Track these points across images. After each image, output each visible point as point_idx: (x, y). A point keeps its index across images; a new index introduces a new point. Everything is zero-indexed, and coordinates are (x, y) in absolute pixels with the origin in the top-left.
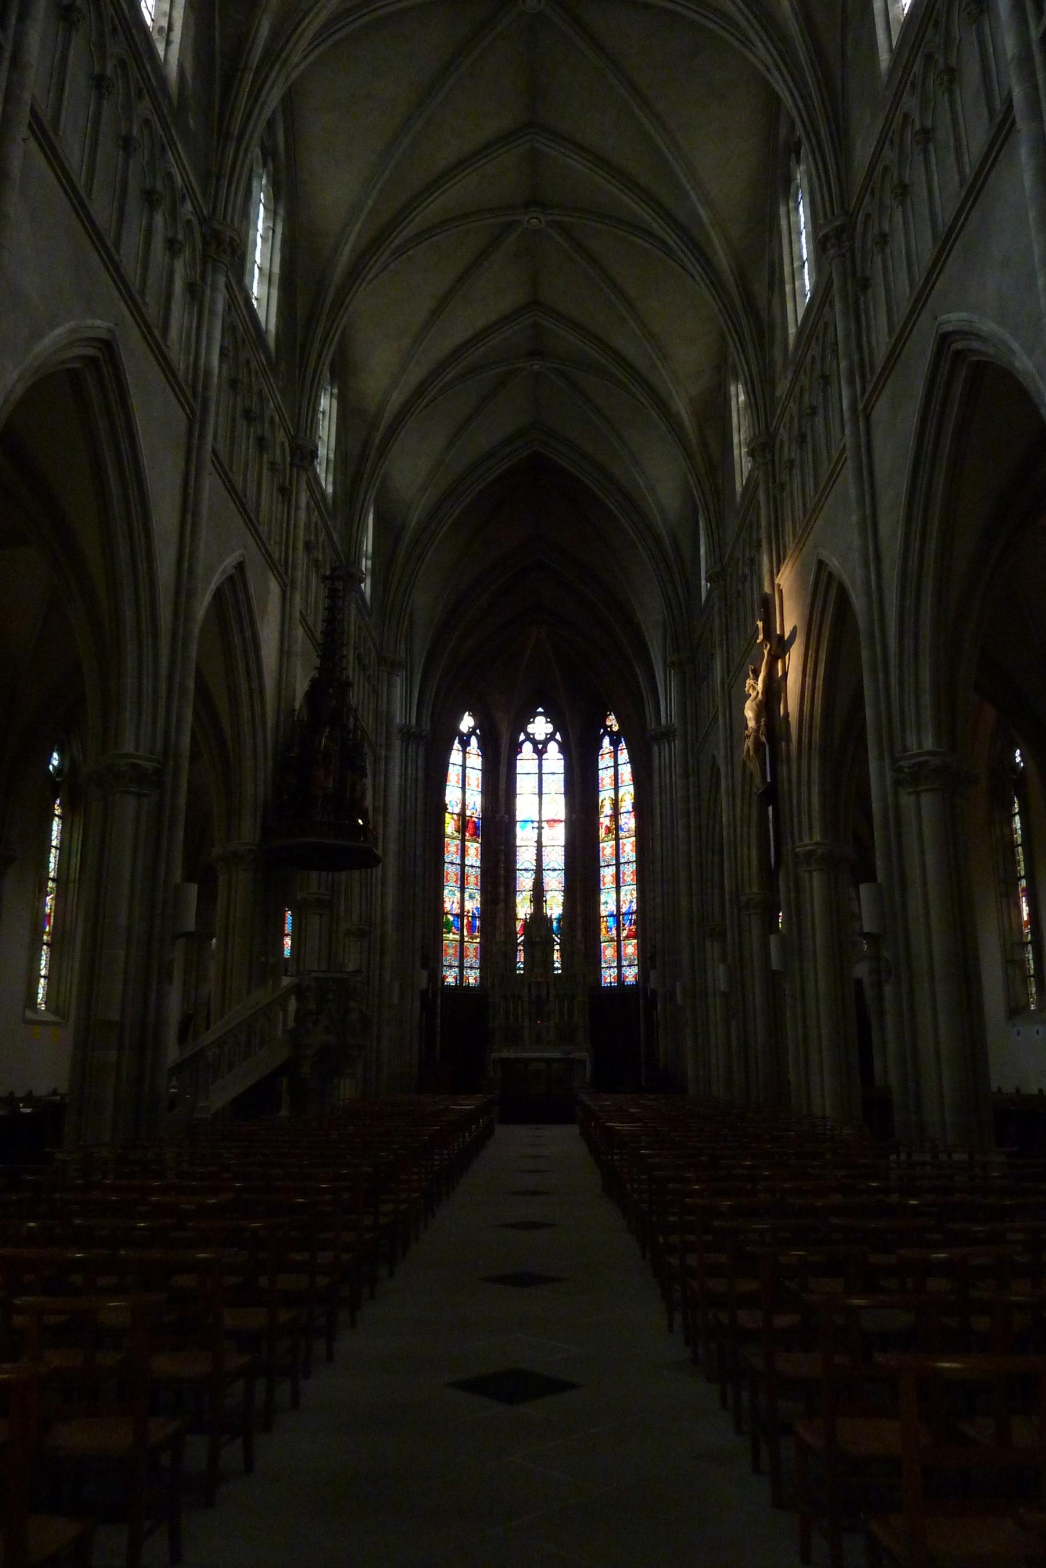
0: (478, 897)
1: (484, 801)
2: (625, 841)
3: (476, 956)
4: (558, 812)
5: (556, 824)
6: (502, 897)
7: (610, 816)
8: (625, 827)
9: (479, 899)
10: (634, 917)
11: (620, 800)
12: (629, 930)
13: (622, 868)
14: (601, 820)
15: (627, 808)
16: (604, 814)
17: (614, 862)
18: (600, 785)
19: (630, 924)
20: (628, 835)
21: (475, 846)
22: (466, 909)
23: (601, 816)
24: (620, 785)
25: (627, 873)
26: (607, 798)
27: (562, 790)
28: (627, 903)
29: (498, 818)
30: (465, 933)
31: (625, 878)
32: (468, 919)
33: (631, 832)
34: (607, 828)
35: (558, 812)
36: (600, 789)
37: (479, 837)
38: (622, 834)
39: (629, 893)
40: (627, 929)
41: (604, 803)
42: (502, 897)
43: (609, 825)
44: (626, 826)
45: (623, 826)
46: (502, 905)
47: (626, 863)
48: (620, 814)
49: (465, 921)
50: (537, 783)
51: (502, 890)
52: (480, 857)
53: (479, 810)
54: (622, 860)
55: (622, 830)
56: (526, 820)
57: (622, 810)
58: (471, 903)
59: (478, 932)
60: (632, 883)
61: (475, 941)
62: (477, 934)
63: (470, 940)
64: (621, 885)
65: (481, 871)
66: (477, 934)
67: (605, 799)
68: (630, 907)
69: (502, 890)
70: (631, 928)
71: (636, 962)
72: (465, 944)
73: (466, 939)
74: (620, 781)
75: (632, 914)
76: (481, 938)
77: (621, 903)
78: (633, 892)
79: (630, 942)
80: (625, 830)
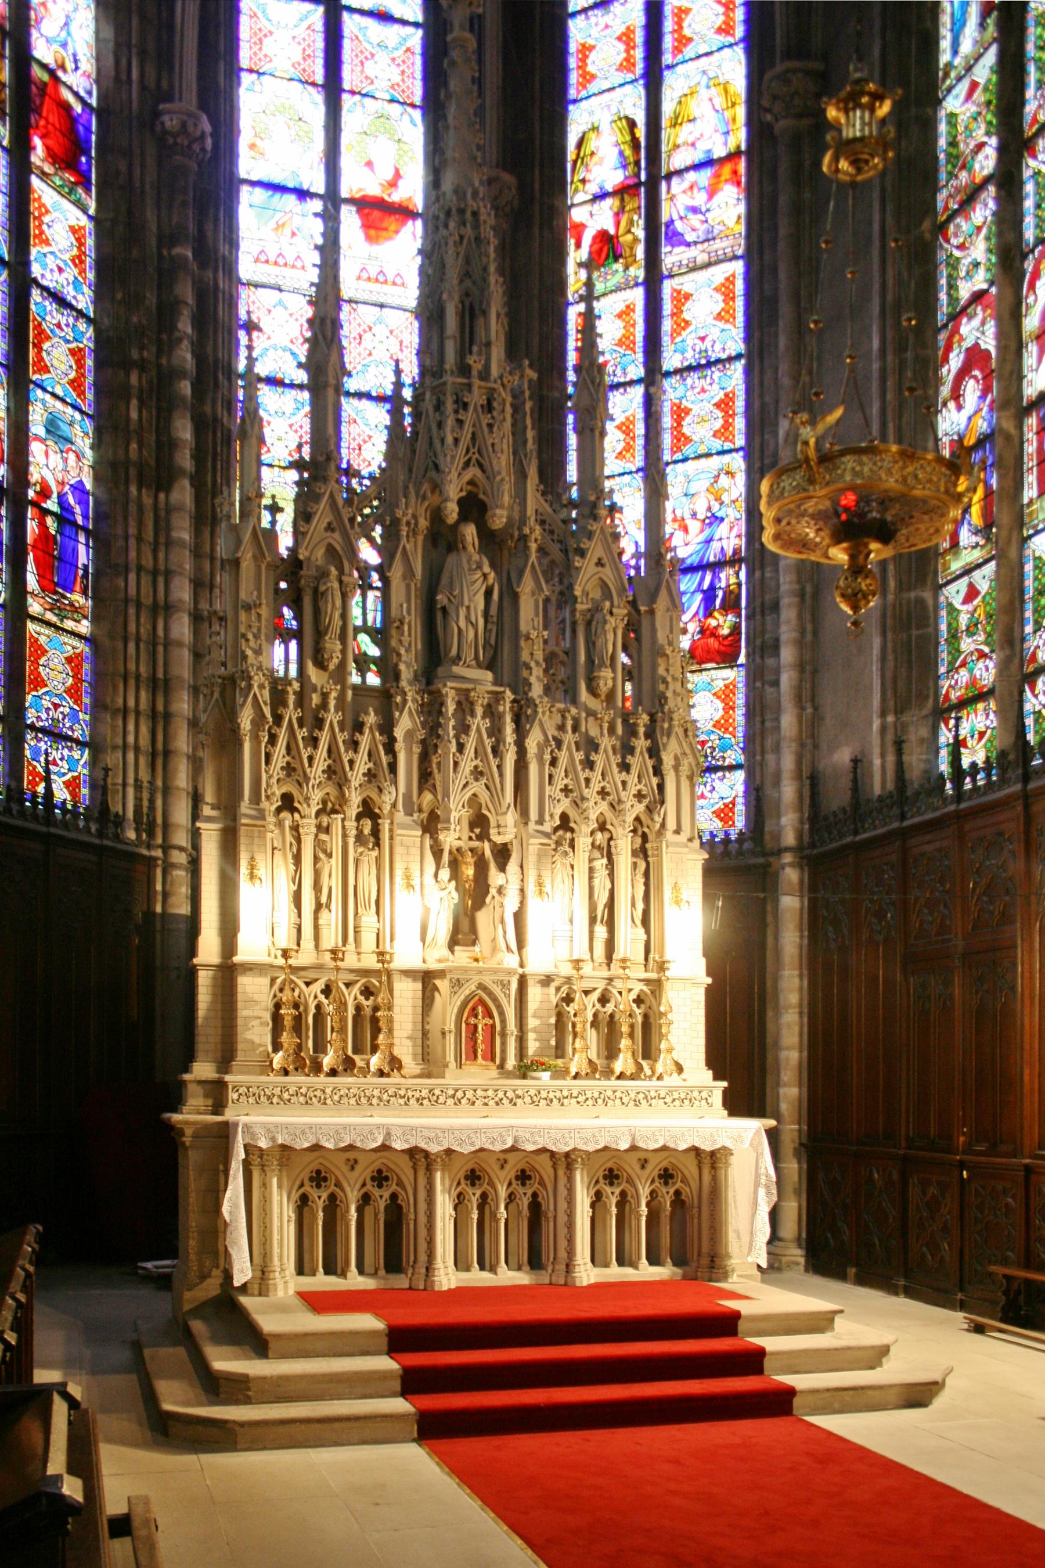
0: (84, 444)
1: (109, 33)
2: (687, 283)
3: (74, 692)
4: (398, 175)
5: (391, 222)
6: (185, 460)
7: (623, 191)
8: (689, 228)
9: (89, 453)
10: (727, 577)
11: (665, 122)
12: (703, 631)
13: (672, 390)
14: (577, 215)
15: (702, 146)
16: (592, 188)
17: (637, 371)
18: (573, 78)
19: (708, 610)
20: (702, 258)
21: (73, 222)
22: (35, 476)
23: (579, 198)
24: (667, 59)
25: (695, 409)
26: (605, 127)
27: (417, 92)
28: (694, 526)
29: (170, 122)
30: (32, 581)
31: (686, 430)
32: (42, 525)
33: (718, 245)
34: (604, 238)
35: (398, 175)
36: (572, 93)
37: (88, 190)
38: (671, 257)
39: (700, 485)
40: (693, 627)
41: (591, 145)
42: (185, 460)
43: (612, 232)
44: (695, 220)
45: (679, 226)
46: (183, 494)
47: (690, 368)
48: (669, 176)
49: (32, 527)
50: (320, 44)
51: (184, 430)
52: (91, 276)
53: (87, 65)
54: (670, 360)
55: (676, 239)
56: (277, 179)
57: (679, 160)
58: (55, 460)
59: (84, 592)
60: (717, 445)
61: (69, 624)
62: (77, 598)
63: (50, 616)
64: (667, 457)
65: (98, 339)
66: (77, 598)
67: (595, 129)
68: (708, 541)
69: (184, 430)
70: (713, 623)
71: (735, 756)
72: (31, 626)
73: (35, 607)
74: (668, 42)
75: (716, 567)
76: (96, 620)
77: (668, 529)
78: (724, 481)
79: (705, 676)
80: (690, 237)
